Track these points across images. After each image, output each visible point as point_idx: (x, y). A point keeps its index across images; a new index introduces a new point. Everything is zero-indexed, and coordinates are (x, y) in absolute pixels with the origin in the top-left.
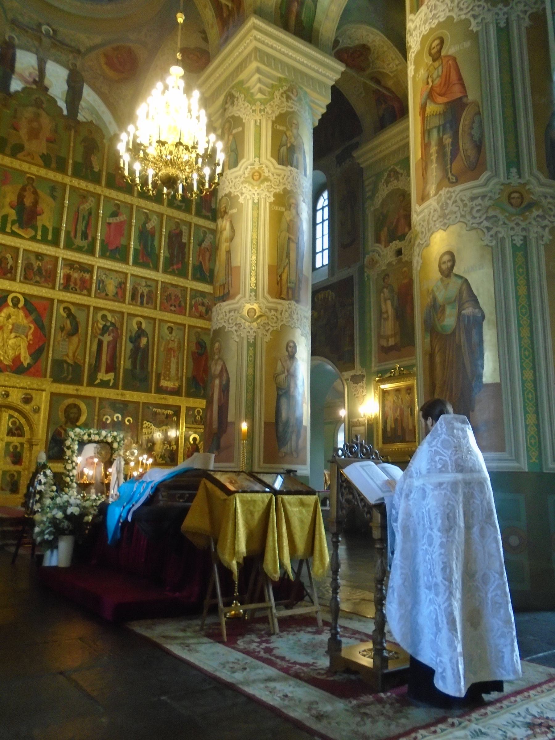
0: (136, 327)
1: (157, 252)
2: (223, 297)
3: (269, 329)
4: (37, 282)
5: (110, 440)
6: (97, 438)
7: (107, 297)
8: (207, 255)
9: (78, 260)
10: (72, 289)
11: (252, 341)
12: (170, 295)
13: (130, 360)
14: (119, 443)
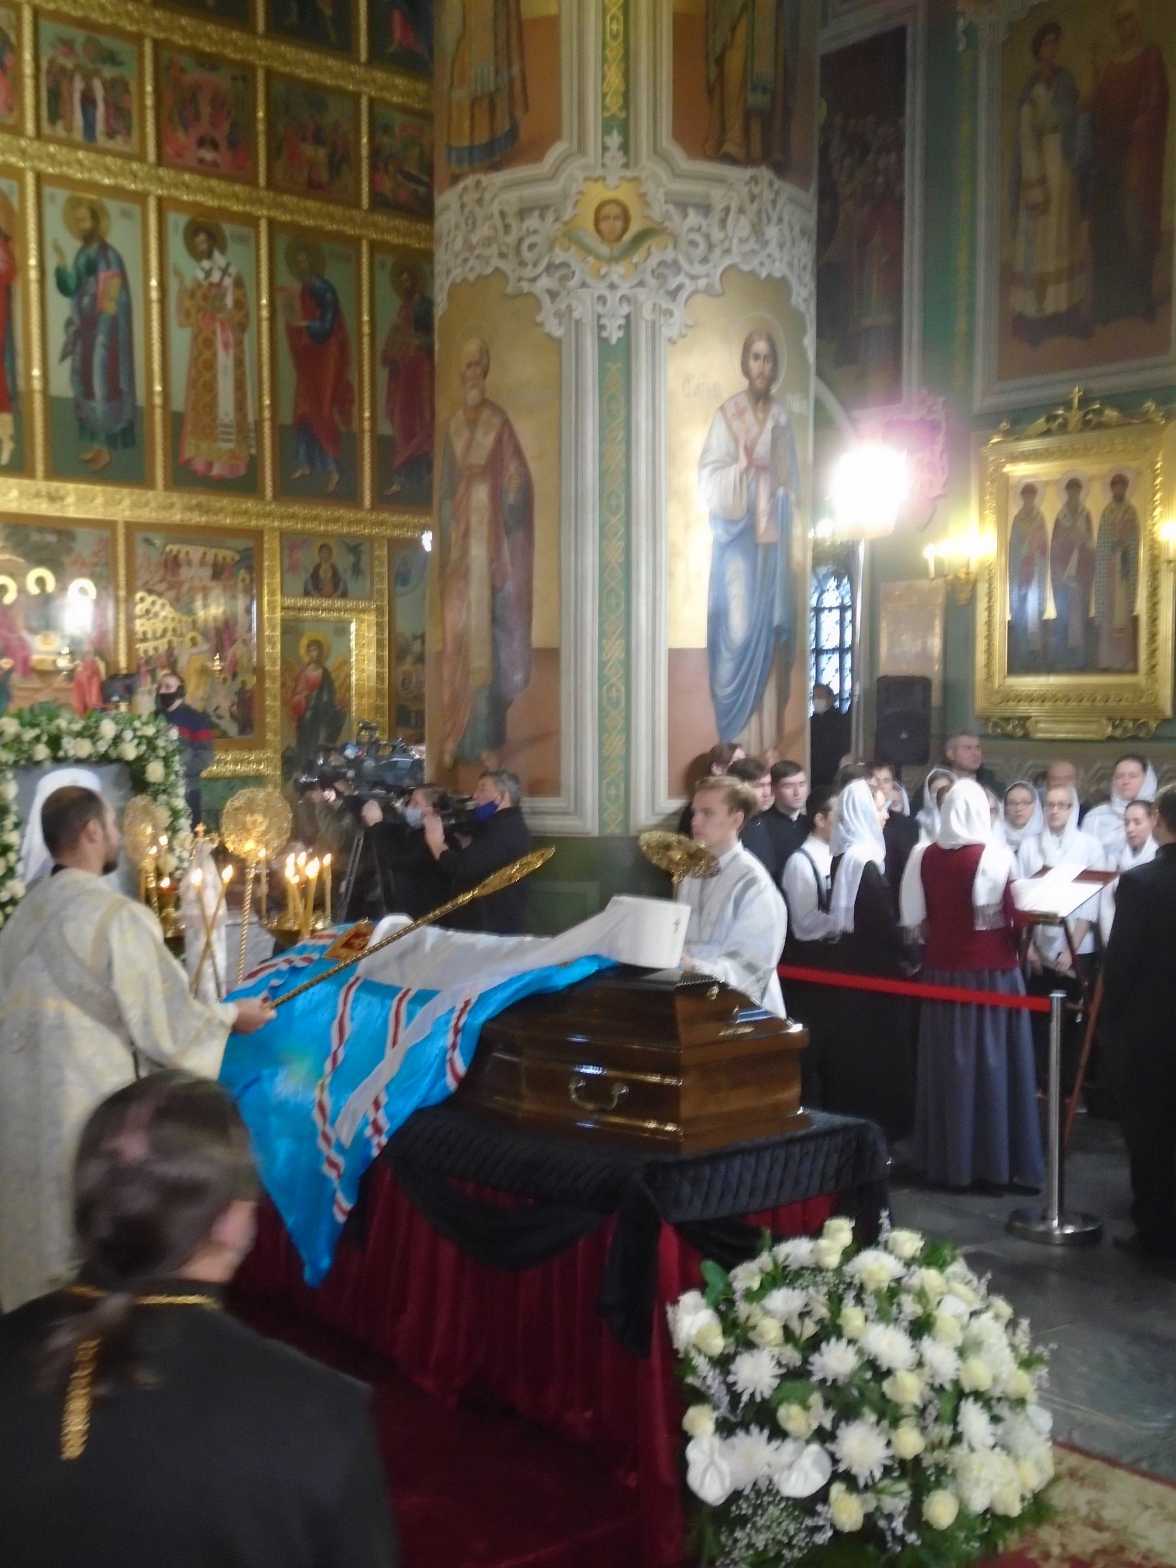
2: (490, 147)
3: (680, 287)
5: (130, 752)
6: (84, 748)
11: (615, 335)
13: (68, 363)
14: (167, 762)
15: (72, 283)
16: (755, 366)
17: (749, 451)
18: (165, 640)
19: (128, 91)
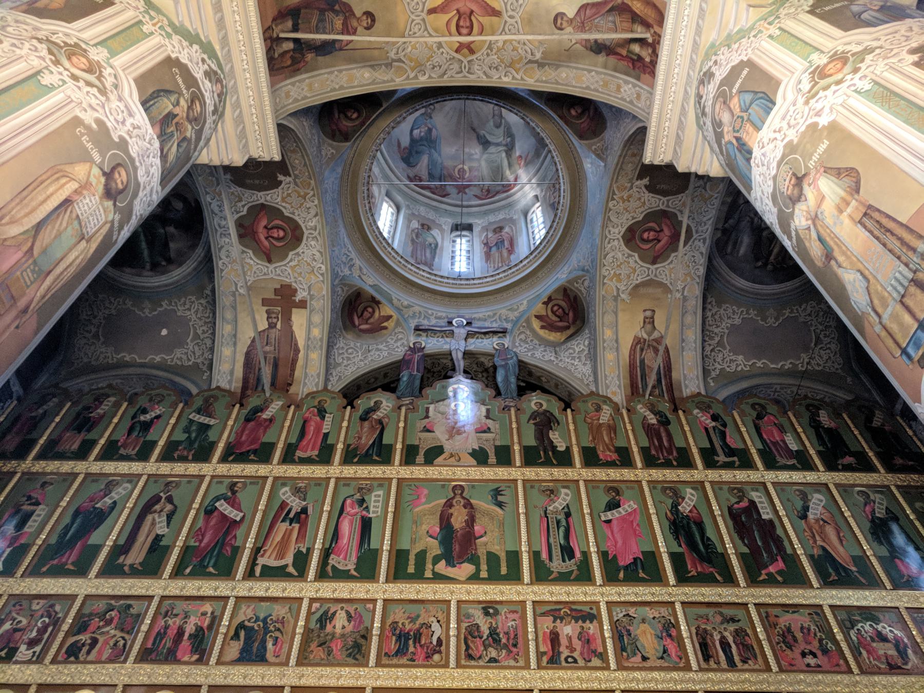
1: (720, 550)
4: (493, 660)
7: (647, 664)
9: (564, 598)
10: (566, 660)
19: (747, 635)
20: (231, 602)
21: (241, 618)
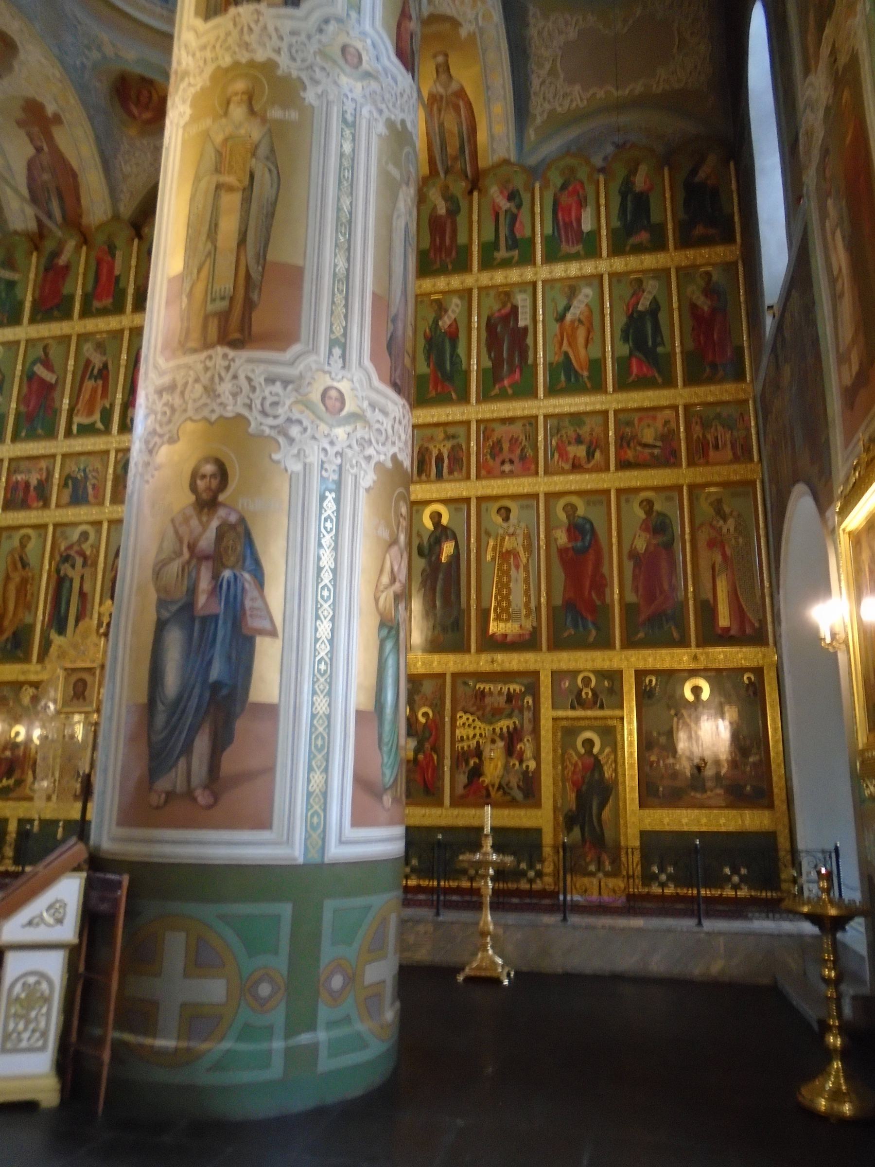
0: (429, 524)
8: (581, 333)
12: (499, 442)
15: (426, 551)
16: (201, 484)
17: (192, 547)
18: (475, 742)
20: (59, 459)
21: (67, 471)
